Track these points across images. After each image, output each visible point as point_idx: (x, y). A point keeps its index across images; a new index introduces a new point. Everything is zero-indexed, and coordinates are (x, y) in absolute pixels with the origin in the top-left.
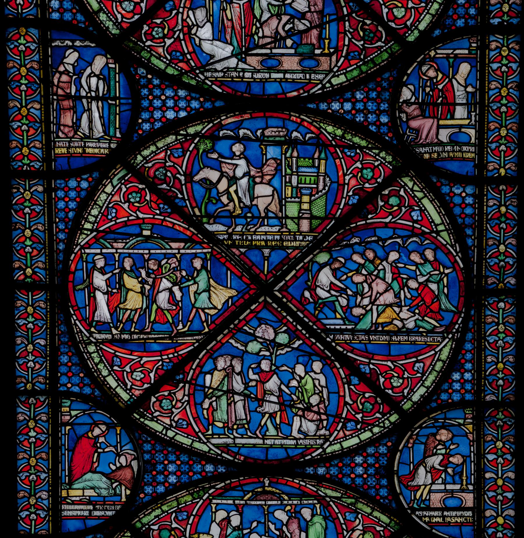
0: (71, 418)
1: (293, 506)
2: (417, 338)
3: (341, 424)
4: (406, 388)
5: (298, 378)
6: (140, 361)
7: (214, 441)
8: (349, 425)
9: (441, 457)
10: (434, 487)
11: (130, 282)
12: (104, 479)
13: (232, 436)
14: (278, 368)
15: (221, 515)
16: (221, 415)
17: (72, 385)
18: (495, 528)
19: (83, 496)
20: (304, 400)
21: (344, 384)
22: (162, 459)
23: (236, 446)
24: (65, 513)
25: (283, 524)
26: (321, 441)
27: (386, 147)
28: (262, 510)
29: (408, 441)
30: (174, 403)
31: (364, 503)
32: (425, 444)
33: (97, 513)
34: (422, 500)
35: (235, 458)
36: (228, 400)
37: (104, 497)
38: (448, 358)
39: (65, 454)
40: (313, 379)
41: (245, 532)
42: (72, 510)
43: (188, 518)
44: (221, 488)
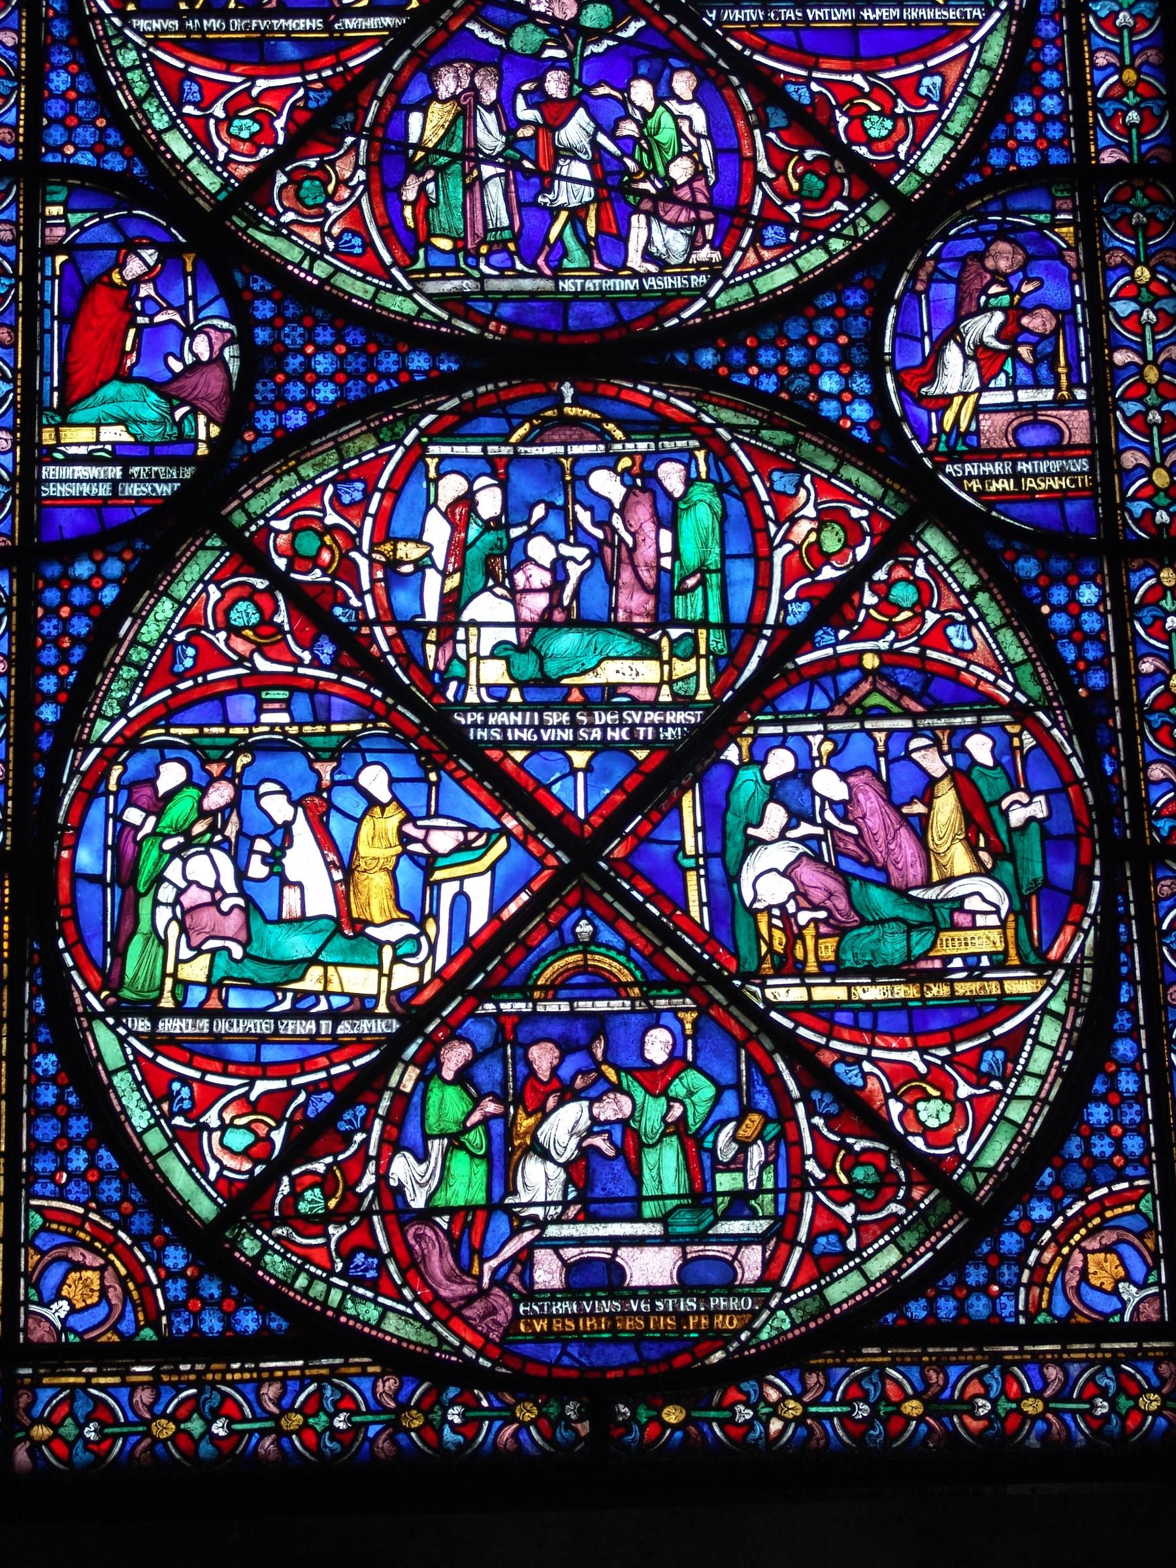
0: (69, 232)
1: (638, 458)
2: (922, 12)
3: (749, 233)
4: (902, 141)
5: (638, 116)
6: (249, 89)
7: (432, 287)
8: (771, 234)
9: (999, 317)
10: (988, 399)
12: (153, 397)
13: (476, 274)
14: (587, 89)
15: (452, 487)
16: (448, 217)
17: (78, 149)
18: (1149, 500)
19: (98, 442)
20: (655, 171)
21: (751, 128)
22: (299, 341)
23: (486, 300)
24: (49, 490)
25: (612, 510)
26: (703, 279)
28: (557, 470)
29: (914, 277)
30: (331, 188)
31: (816, 445)
32: (958, 282)
33: (133, 490)
34: (959, 434)
35: (484, 328)
36: (464, 175)
37: (152, 445)
38: (1002, 60)
39: (51, 331)
40: (676, 118)
41: (515, 532)
42: (67, 481)
43: (367, 498)
44: (452, 411)
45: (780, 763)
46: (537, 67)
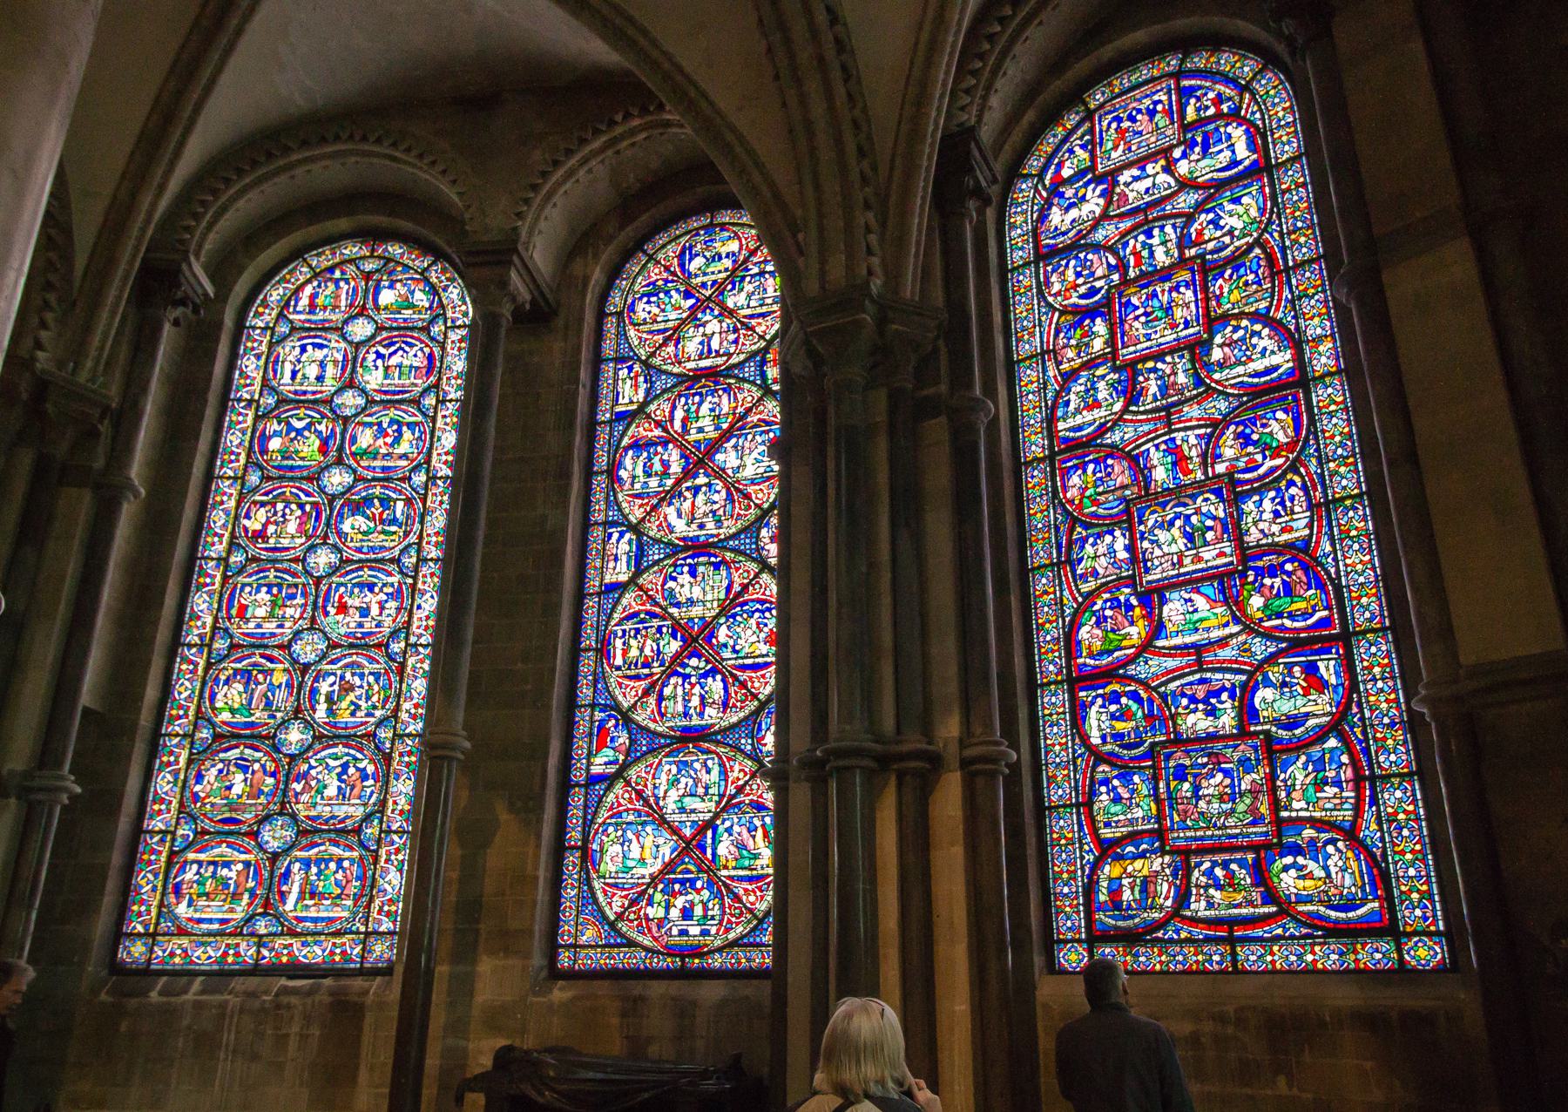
11: (633, 642)
16: (670, 710)
27: (754, 560)
45: (728, 824)
46: (689, 676)
